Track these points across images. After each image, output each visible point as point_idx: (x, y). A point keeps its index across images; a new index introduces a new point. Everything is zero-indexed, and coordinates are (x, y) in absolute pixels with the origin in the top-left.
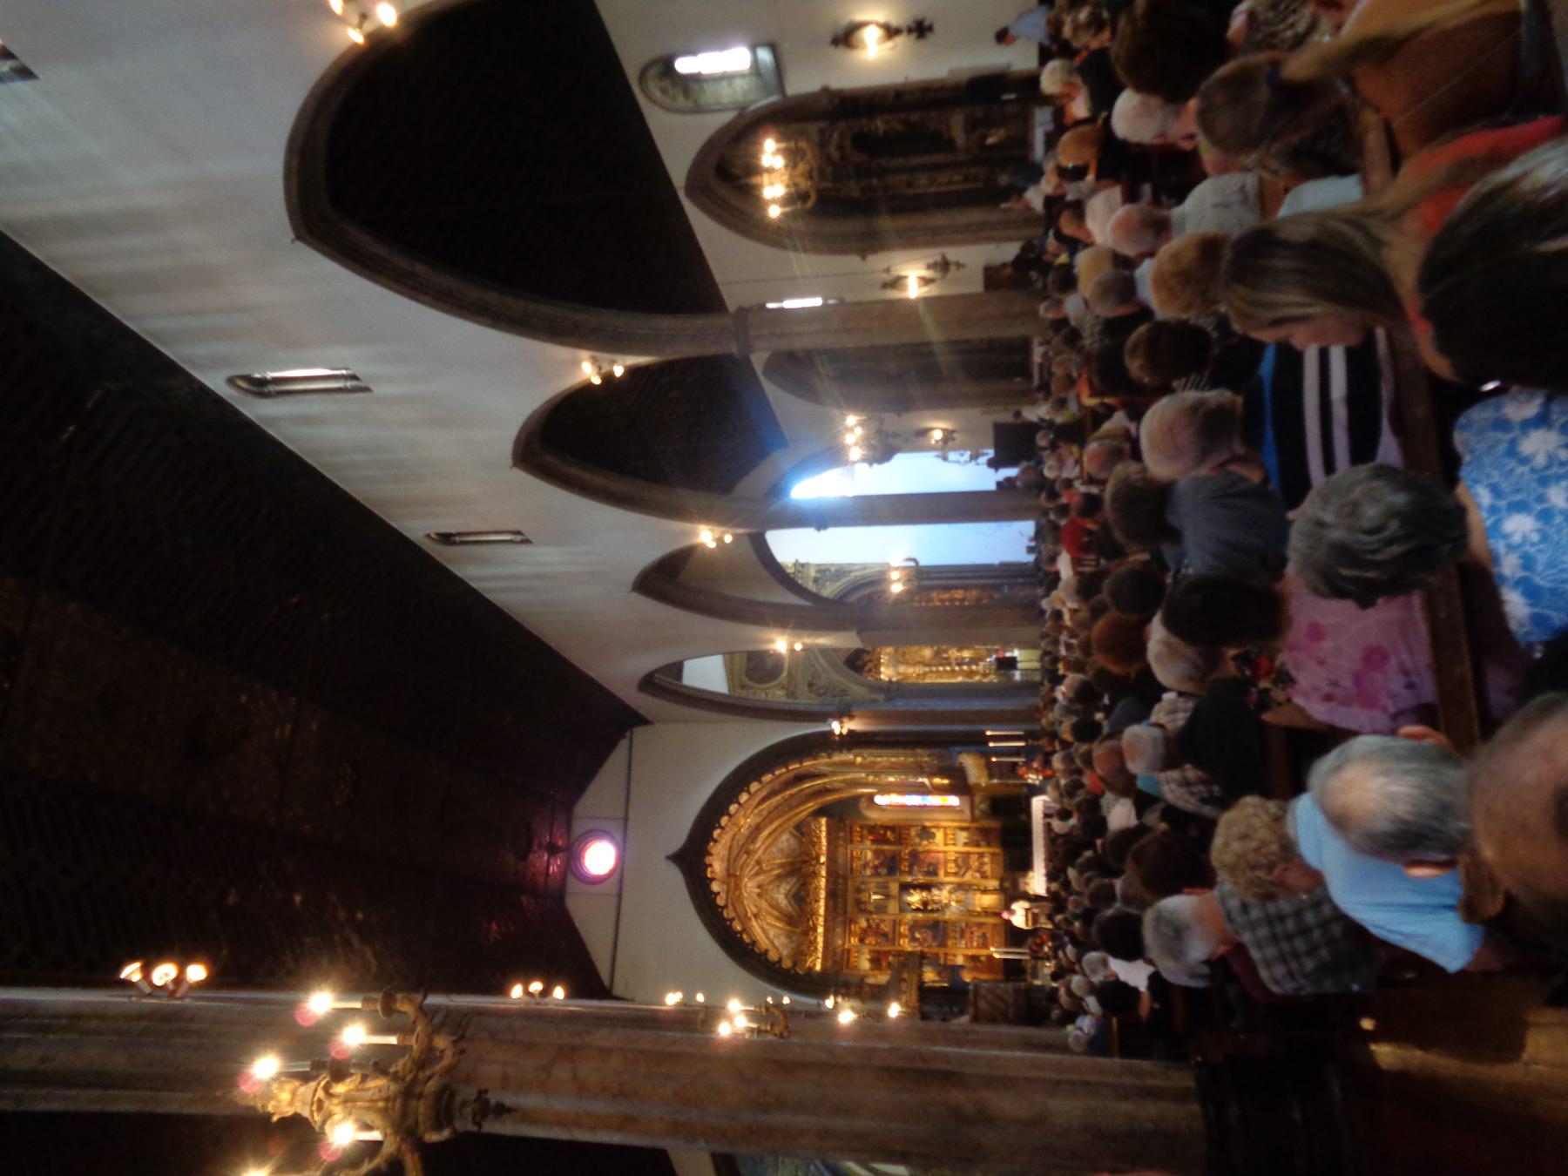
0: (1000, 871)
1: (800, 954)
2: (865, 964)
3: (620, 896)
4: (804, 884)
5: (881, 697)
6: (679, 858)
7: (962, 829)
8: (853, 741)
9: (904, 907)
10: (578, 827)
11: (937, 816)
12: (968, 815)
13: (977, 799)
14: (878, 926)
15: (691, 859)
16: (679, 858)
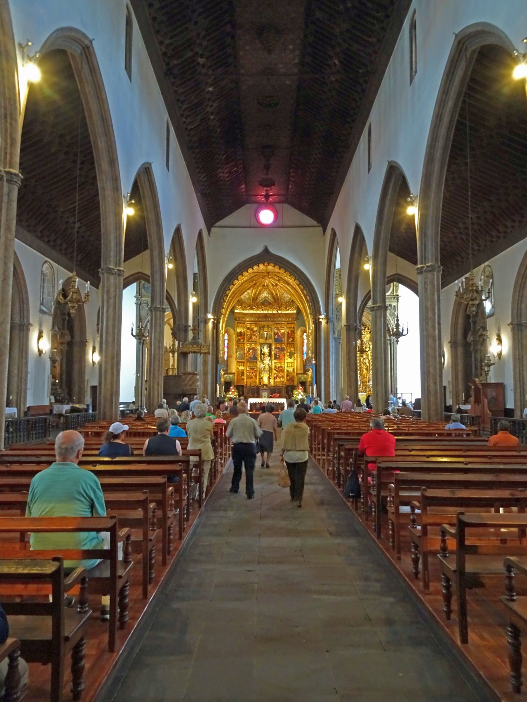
1: (241, 303)
2: (239, 330)
3: (251, 227)
4: (270, 304)
5: (336, 335)
6: (266, 250)
7: (294, 369)
8: (317, 324)
9: (262, 345)
10: (279, 206)
13: (305, 376)
14: (254, 335)
15: (266, 256)
16: (266, 250)
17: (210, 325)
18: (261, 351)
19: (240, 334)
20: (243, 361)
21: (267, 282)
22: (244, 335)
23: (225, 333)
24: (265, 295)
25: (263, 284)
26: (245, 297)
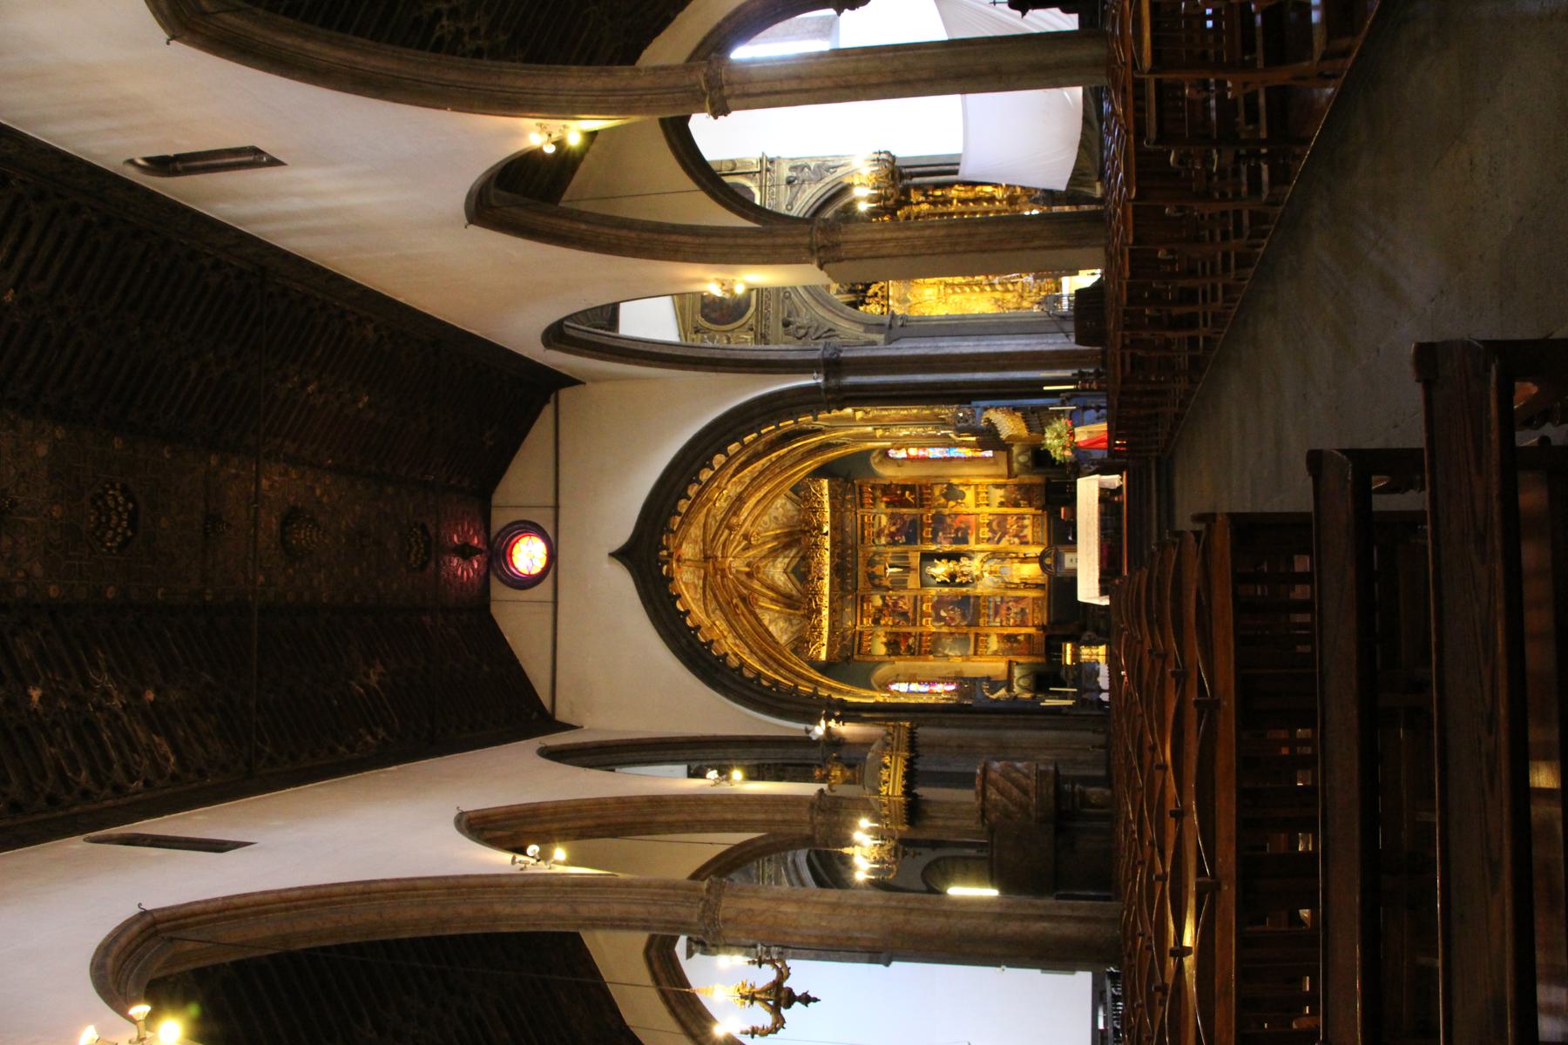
0: (1043, 535)
1: (801, 644)
2: (880, 649)
3: (555, 603)
4: (803, 558)
5: (880, 338)
6: (623, 555)
10: (499, 520)
11: (967, 470)
12: (1004, 470)
13: (1015, 450)
14: (895, 604)
15: (644, 556)
16: (623, 555)
17: (847, 729)
18: (944, 583)
19: (894, 646)
20: (972, 638)
21: (737, 564)
22: (897, 634)
23: (888, 691)
24: (778, 572)
25: (743, 578)
26: (784, 631)
